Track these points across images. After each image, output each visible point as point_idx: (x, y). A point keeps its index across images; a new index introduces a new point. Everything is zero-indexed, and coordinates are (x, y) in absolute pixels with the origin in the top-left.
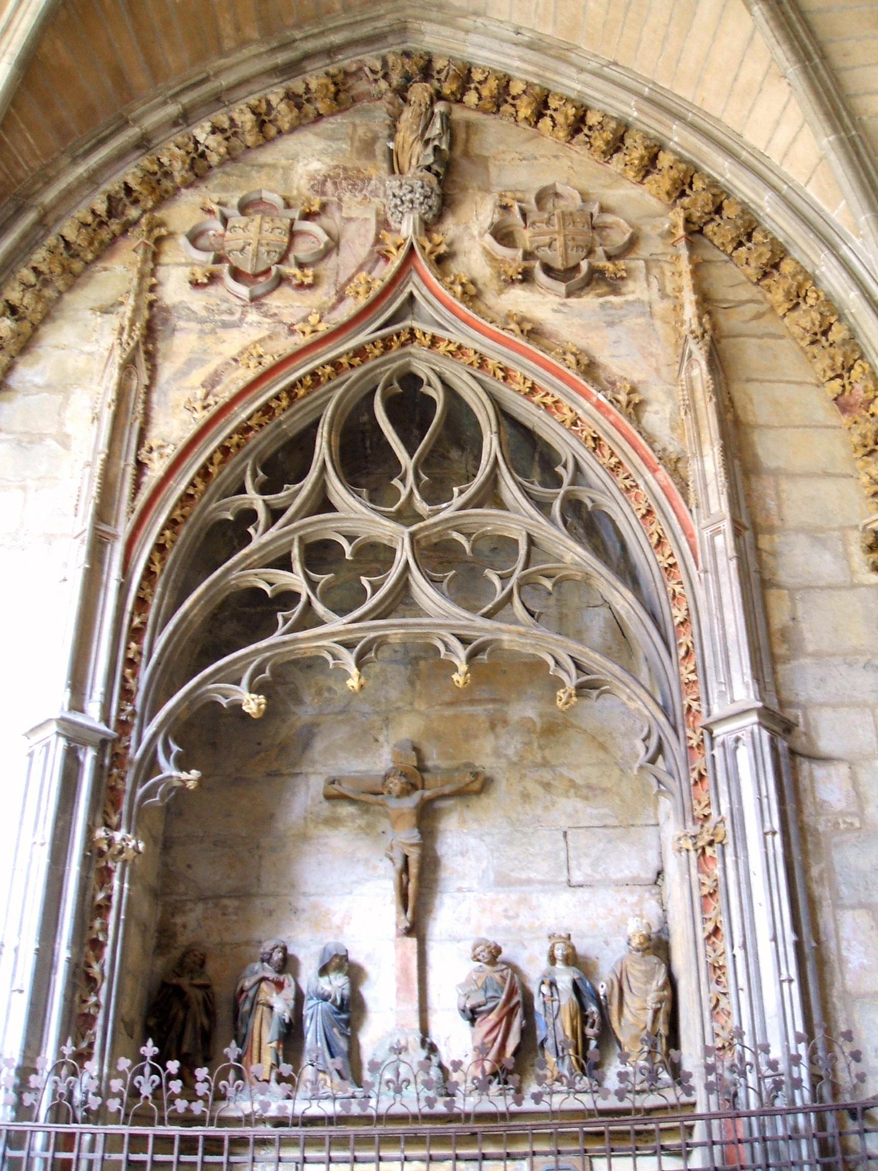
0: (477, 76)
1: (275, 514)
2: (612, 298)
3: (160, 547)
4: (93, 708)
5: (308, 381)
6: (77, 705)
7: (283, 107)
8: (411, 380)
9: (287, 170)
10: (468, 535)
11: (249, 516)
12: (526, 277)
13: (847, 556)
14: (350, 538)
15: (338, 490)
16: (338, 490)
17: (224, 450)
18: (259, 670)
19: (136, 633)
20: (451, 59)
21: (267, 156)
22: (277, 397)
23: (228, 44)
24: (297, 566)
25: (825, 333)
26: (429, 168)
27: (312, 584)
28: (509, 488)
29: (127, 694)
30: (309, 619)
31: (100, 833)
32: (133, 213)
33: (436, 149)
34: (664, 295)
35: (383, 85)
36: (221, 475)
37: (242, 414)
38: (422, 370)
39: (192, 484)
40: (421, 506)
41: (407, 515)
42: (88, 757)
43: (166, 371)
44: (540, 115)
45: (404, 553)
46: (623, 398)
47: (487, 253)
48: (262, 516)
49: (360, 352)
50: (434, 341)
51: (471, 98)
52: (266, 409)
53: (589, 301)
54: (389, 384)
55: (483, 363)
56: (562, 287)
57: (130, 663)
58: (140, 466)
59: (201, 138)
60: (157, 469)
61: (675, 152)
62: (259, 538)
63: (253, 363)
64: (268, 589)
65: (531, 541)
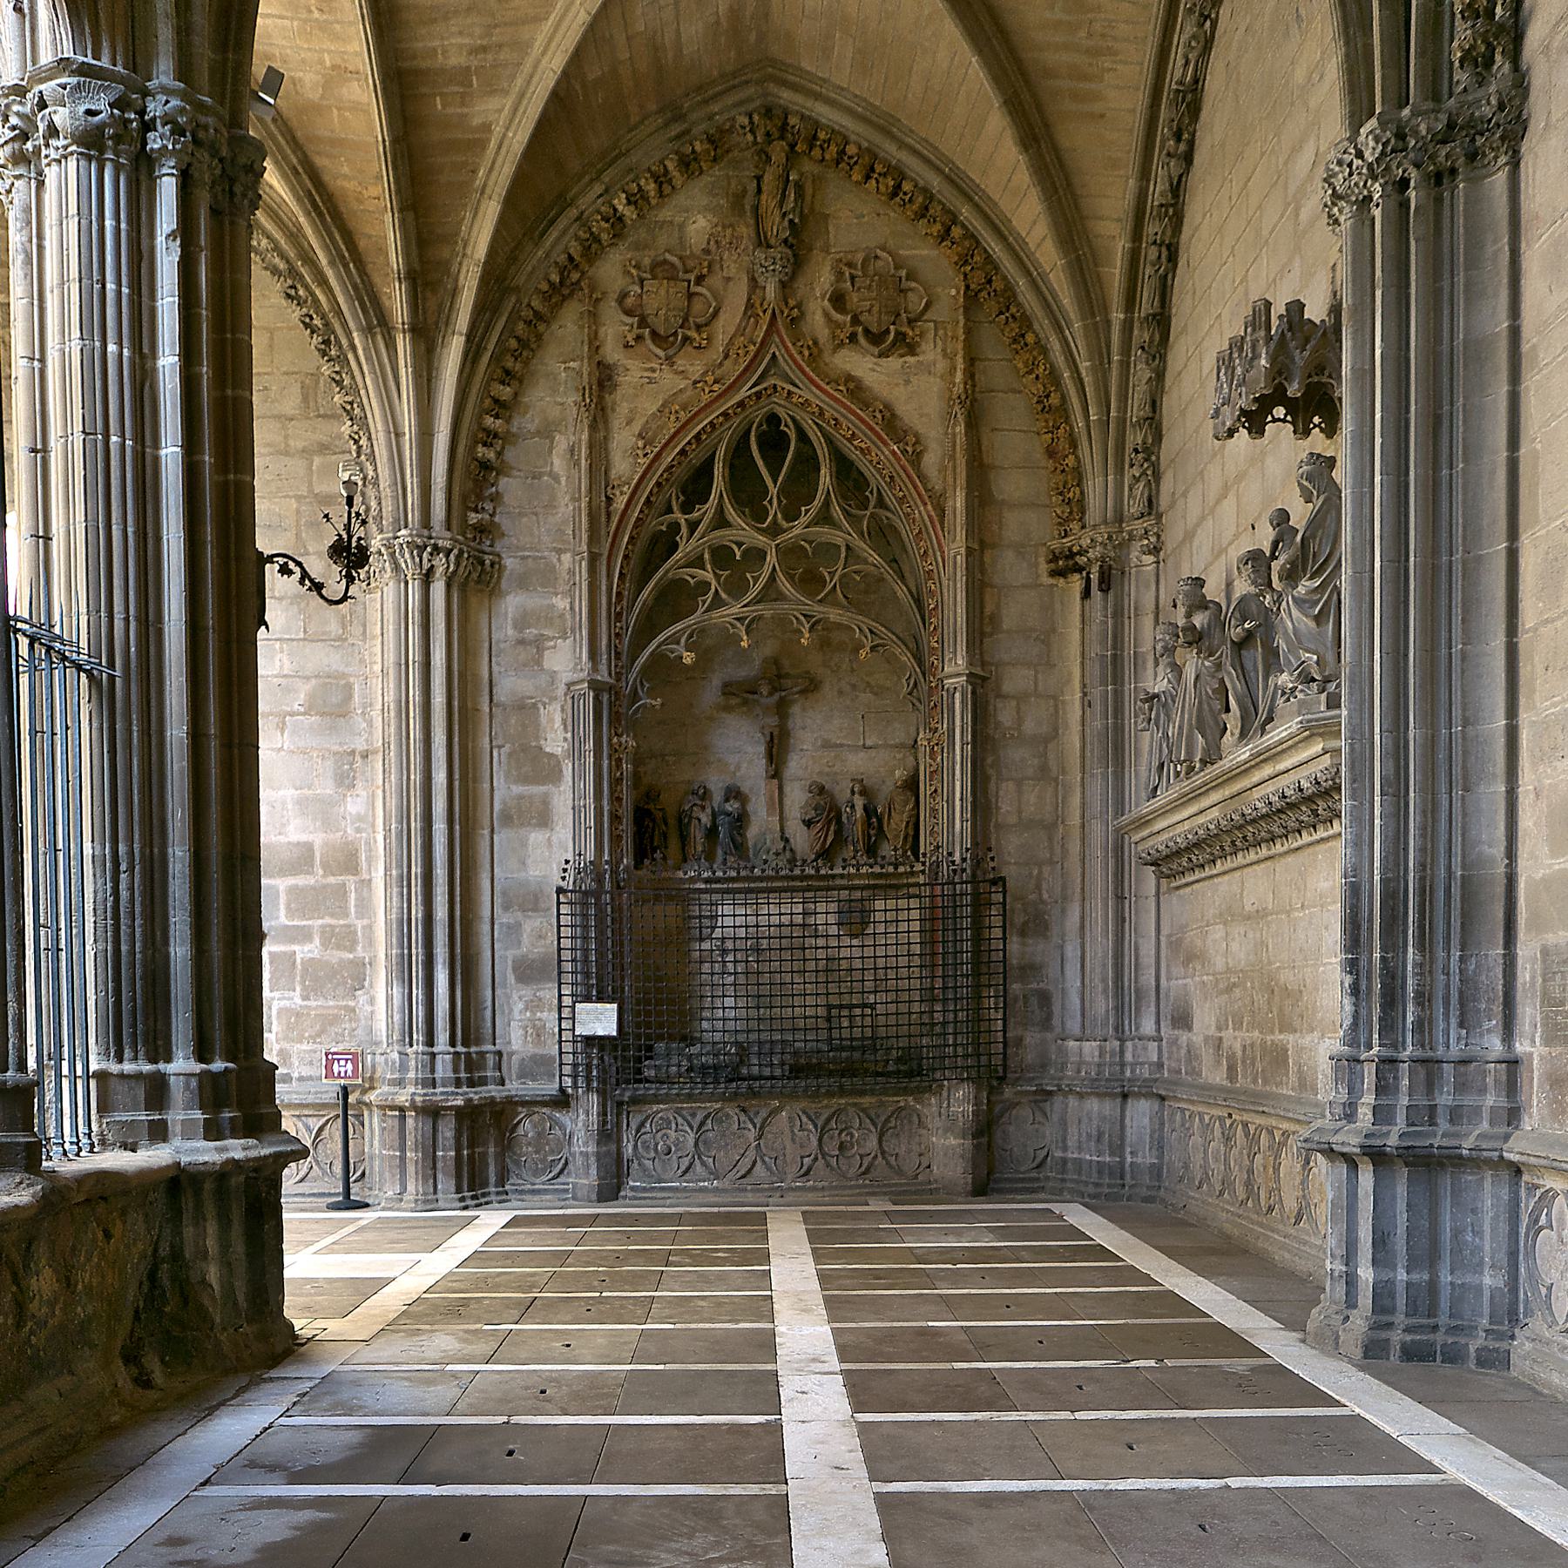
0: (822, 135)
1: (693, 527)
2: (910, 359)
3: (626, 557)
4: (603, 668)
5: (709, 429)
6: (595, 669)
7: (676, 173)
8: (773, 419)
9: (682, 226)
10: (810, 543)
11: (675, 528)
12: (853, 338)
13: (1036, 565)
14: (739, 544)
15: (731, 513)
16: (731, 513)
17: (658, 484)
18: (691, 636)
19: (619, 615)
20: (803, 117)
21: (665, 214)
22: (689, 443)
23: (634, 119)
24: (709, 567)
25: (1047, 396)
26: (785, 241)
27: (717, 577)
28: (837, 512)
29: (618, 655)
30: (717, 602)
31: (615, 740)
32: (575, 276)
33: (791, 221)
34: (945, 355)
35: (750, 137)
36: (659, 501)
37: (668, 459)
38: (782, 413)
39: (641, 511)
40: (785, 525)
41: (775, 530)
42: (605, 698)
43: (617, 422)
44: (868, 177)
45: (771, 558)
46: (910, 449)
47: (826, 315)
48: (684, 530)
49: (741, 404)
50: (789, 393)
51: (816, 152)
52: (683, 452)
53: (894, 363)
54: (760, 425)
55: (821, 414)
56: (876, 351)
57: (617, 635)
58: (609, 500)
59: (620, 208)
60: (620, 502)
61: (964, 226)
62: (686, 547)
63: (673, 418)
64: (692, 581)
65: (848, 548)
